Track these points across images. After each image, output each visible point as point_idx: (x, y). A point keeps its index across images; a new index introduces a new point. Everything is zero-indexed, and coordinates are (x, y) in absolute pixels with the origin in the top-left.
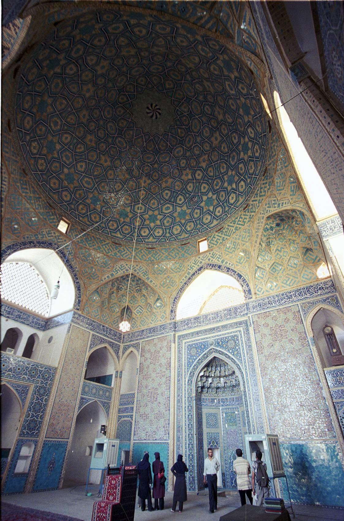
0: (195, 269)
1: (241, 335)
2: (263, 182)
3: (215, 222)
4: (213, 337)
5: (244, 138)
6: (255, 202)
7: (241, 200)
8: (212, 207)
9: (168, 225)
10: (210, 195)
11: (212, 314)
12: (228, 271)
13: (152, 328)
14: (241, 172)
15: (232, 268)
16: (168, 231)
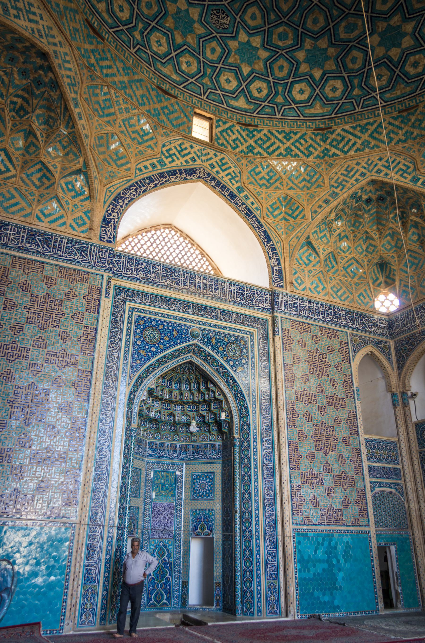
0: (177, 162)
1: (252, 341)
2: (392, 121)
3: (241, 103)
4: (199, 322)
5: (405, 20)
6: (351, 137)
7: (317, 109)
8: (249, 69)
9: (146, 11)
10: (256, 41)
11: (205, 278)
12: (247, 214)
13: (40, 233)
14: (350, 66)
15: (257, 213)
16: (140, 26)
